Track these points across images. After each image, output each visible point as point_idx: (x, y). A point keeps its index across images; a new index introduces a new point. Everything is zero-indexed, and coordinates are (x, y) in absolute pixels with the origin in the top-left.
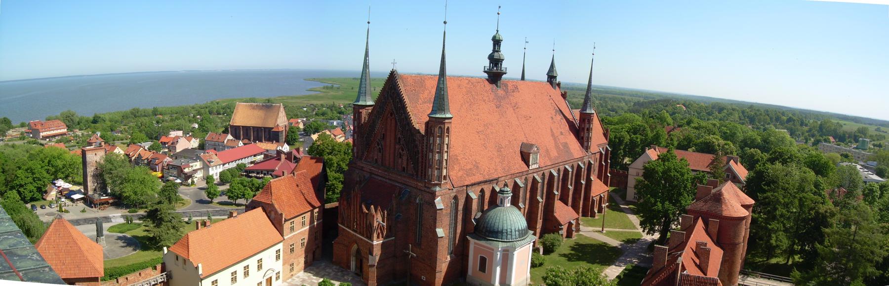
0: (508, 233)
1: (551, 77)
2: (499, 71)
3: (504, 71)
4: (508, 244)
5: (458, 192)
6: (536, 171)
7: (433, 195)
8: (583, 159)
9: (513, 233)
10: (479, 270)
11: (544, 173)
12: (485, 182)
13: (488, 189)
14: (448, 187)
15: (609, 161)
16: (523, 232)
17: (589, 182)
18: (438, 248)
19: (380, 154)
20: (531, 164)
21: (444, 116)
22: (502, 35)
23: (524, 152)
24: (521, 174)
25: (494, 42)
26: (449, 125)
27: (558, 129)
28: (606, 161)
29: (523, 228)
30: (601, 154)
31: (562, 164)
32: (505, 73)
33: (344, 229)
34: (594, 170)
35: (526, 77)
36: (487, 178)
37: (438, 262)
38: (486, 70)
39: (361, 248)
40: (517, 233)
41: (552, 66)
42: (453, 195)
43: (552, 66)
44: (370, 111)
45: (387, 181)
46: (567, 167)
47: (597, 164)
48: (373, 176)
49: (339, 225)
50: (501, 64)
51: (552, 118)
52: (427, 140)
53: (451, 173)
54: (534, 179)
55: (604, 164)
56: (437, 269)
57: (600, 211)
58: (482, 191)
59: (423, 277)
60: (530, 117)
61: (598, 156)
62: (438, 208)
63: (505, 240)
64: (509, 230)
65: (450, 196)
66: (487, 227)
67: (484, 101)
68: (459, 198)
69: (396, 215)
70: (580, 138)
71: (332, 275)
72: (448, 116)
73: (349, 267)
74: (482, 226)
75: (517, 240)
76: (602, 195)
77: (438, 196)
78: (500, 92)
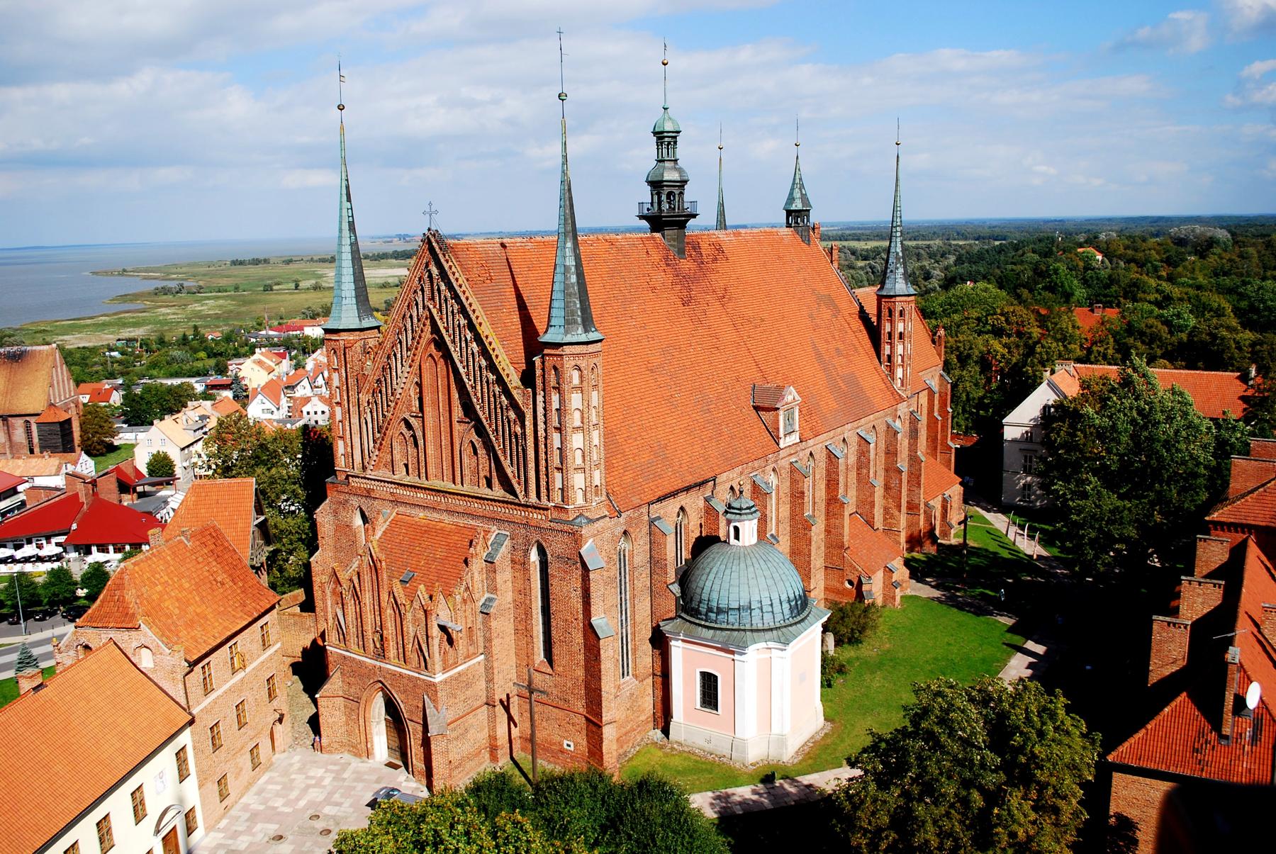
0: (764, 611)
1: (796, 217)
8: (896, 410)
9: (777, 608)
14: (607, 513)
18: (603, 667)
20: (781, 434)
24: (762, 462)
25: (659, 138)
26: (595, 360)
27: (827, 341)
28: (943, 412)
29: (797, 594)
32: (694, 216)
33: (345, 657)
36: (691, 480)
38: (646, 212)
40: (786, 606)
41: (797, 183)
43: (797, 183)
45: (446, 518)
48: (402, 509)
50: (681, 193)
51: (811, 316)
52: (544, 402)
55: (940, 418)
59: (566, 742)
60: (763, 320)
63: (760, 626)
64: (766, 602)
66: (709, 600)
69: (483, 601)
70: (883, 358)
71: (326, 782)
72: (593, 336)
73: (369, 754)
74: (697, 598)
78: (686, 265)
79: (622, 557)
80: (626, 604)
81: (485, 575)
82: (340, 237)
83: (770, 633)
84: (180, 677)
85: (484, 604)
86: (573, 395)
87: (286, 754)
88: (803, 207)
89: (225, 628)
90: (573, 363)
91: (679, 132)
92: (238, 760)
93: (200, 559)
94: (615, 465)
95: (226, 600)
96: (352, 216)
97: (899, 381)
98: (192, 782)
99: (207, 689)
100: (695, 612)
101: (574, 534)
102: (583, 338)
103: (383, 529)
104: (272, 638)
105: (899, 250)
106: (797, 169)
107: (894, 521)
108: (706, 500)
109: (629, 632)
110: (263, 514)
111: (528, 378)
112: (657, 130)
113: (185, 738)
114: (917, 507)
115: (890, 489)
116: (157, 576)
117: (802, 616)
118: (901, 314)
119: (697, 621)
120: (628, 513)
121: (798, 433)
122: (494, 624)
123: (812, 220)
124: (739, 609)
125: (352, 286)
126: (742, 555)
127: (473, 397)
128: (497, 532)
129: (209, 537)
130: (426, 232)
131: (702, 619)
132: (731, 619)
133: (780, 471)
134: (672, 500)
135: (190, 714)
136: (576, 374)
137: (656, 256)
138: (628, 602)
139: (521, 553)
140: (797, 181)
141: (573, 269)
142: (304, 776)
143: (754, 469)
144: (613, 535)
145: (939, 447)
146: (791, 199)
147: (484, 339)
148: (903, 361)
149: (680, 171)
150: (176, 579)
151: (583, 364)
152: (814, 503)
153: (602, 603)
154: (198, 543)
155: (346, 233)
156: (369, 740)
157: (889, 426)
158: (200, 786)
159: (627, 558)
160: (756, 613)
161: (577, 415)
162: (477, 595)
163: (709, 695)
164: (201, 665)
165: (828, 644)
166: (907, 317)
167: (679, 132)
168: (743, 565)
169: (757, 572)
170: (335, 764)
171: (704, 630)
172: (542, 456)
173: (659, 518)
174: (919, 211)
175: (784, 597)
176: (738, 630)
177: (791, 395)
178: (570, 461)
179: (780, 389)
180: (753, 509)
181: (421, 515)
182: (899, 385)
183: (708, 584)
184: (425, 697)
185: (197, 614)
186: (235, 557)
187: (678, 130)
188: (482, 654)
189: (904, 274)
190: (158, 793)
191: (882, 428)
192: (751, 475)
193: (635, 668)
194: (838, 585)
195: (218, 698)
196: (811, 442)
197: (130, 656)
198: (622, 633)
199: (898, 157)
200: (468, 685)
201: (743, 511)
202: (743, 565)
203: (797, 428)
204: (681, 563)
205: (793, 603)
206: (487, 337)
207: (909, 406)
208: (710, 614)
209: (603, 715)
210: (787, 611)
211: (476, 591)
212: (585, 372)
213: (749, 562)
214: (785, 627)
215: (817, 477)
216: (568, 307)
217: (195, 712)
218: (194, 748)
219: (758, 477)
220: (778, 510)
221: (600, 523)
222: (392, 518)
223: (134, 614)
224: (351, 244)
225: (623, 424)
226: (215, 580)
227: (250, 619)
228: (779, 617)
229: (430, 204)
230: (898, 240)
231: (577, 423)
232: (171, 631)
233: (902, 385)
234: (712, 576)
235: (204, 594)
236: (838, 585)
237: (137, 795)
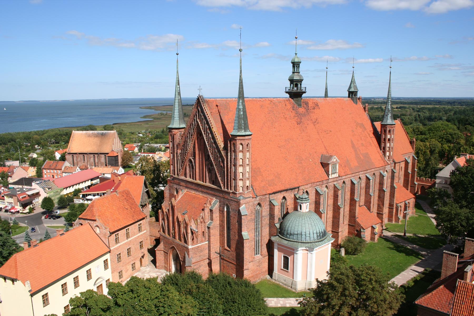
0: (307, 236)
1: (352, 94)
2: (299, 91)
3: (304, 90)
4: (307, 245)
5: (261, 199)
6: (336, 179)
7: (238, 203)
8: (385, 168)
9: (312, 235)
10: (283, 268)
11: (344, 181)
12: (287, 190)
13: (290, 196)
14: (251, 196)
15: (416, 170)
17: (393, 189)
18: (244, 249)
20: (330, 173)
21: (244, 133)
23: (324, 163)
24: (321, 183)
26: (248, 142)
29: (321, 231)
30: (407, 163)
31: (362, 173)
32: (305, 92)
34: (399, 179)
35: (329, 95)
36: (288, 187)
37: (245, 261)
38: (287, 90)
40: (315, 235)
41: (353, 82)
42: (257, 202)
43: (353, 82)
44: (183, 132)
46: (368, 176)
47: (402, 173)
50: (301, 84)
53: (254, 184)
54: (335, 187)
55: (410, 173)
56: (244, 268)
57: (405, 216)
58: (284, 198)
59: (233, 275)
60: (331, 131)
61: (403, 165)
62: (242, 215)
63: (304, 241)
64: (308, 233)
65: (254, 204)
66: (287, 230)
67: (286, 118)
68: (262, 205)
69: (209, 223)
75: (315, 241)
76: (407, 202)
77: (242, 204)
78: (301, 110)
79: (258, 212)
80: (259, 229)
81: (210, 214)
82: (175, 97)
84: (107, 237)
85: (209, 224)
86: (239, 154)
87: (145, 267)
88: (354, 90)
89: (125, 223)
90: (240, 142)
91: (300, 62)
92: (127, 267)
93: (121, 201)
94: (258, 180)
95: (127, 214)
97: (387, 157)
98: (109, 270)
99: (117, 241)
101: (238, 202)
102: (244, 134)
103: (181, 196)
104: (143, 229)
105: (389, 107)
106: (353, 76)
107: (381, 210)
108: (295, 195)
109: (260, 239)
110: (147, 188)
111: (225, 148)
112: (292, 61)
113: (108, 256)
114: (393, 205)
115: (380, 197)
116: (105, 204)
117: (322, 239)
118: (389, 131)
119: (283, 237)
120: (260, 197)
121: (338, 174)
122: (211, 231)
124: (297, 234)
125: (178, 114)
127: (209, 153)
128: (215, 200)
129: (125, 194)
130: (198, 96)
131: (285, 237)
132: (294, 238)
133: (329, 187)
134: (279, 194)
135: (110, 249)
136: (241, 146)
137: (289, 106)
138: (260, 228)
139: (222, 207)
140: (353, 81)
142: (148, 275)
143: (317, 185)
144: (254, 204)
145: (410, 184)
146: (350, 87)
147: (214, 133)
148: (389, 149)
149: (301, 76)
150: (111, 206)
151: (243, 143)
152: (345, 200)
153: (246, 227)
154: (121, 195)
155: (177, 96)
156: (170, 266)
157: (381, 174)
158: (112, 273)
159: (260, 213)
160: (304, 236)
161: (241, 160)
162: (206, 221)
163: (286, 265)
164: (115, 234)
165: (342, 252)
166: (392, 132)
167: (300, 62)
170: (159, 273)
171: (285, 241)
172: (229, 174)
173: (273, 200)
174: (396, 94)
175: (315, 232)
177: (334, 159)
178: (238, 177)
179: (331, 157)
181: (194, 192)
182: (387, 158)
183: (288, 224)
184: (186, 253)
185: (117, 218)
186: (133, 201)
187: (300, 61)
188: (207, 241)
189: (391, 117)
191: (377, 174)
192: (316, 187)
193: (261, 252)
194: (353, 231)
195: (121, 245)
196: (344, 177)
197: (93, 228)
198: (257, 239)
199: (390, 72)
200: (201, 251)
201: (303, 199)
202: (301, 219)
203: (337, 171)
205: (318, 234)
206: (214, 132)
207: (391, 167)
208: (287, 235)
209: (244, 266)
211: (206, 219)
212: (244, 146)
213: (303, 218)
214: (314, 242)
215: (346, 190)
216: (239, 123)
217: (112, 249)
218: (111, 260)
219: (319, 188)
220: (327, 201)
221: (249, 199)
222: (185, 192)
223: (95, 215)
224: (178, 100)
225: (264, 165)
226: (125, 208)
227: (134, 221)
228: (312, 239)
229: (200, 86)
231: (241, 164)
232: (106, 222)
233: (389, 158)
234: (290, 222)
235: (120, 212)
236: (353, 231)
237: (89, 273)
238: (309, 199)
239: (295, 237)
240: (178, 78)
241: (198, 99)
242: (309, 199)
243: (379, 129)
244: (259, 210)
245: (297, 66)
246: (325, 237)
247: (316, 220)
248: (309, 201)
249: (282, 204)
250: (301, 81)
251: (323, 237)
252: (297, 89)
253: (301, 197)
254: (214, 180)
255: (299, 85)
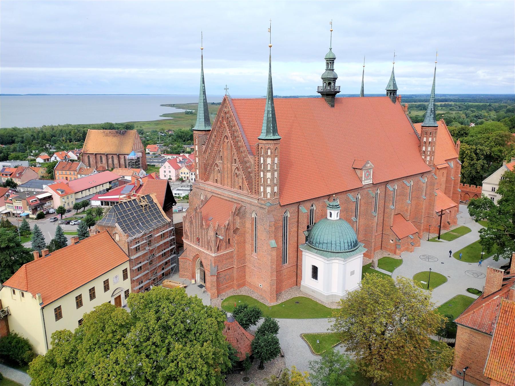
1: (392, 92)
3: (338, 90)
9: (342, 245)
16: (353, 244)
19: (219, 175)
20: (363, 180)
22: (336, 52)
29: (352, 240)
32: (339, 92)
38: (320, 90)
39: (203, 261)
40: (346, 244)
41: (393, 79)
43: (393, 79)
49: (184, 241)
59: (260, 284)
64: (338, 242)
75: (346, 251)
83: (338, 254)
88: (394, 88)
91: (335, 58)
96: (205, 89)
98: (128, 280)
100: (311, 243)
102: (272, 138)
117: (353, 249)
119: (312, 246)
123: (397, 94)
126: (331, 223)
131: (313, 245)
141: (271, 112)
146: (389, 85)
148: (430, 154)
152: (379, 208)
168: (331, 227)
169: (336, 230)
176: (326, 251)
180: (338, 206)
183: (317, 233)
190: (114, 283)
201: (334, 207)
202: (331, 227)
203: (371, 178)
204: (313, 224)
205: (350, 244)
208: (316, 244)
210: (346, 246)
224: (204, 100)
228: (343, 248)
229: (226, 86)
230: (433, 103)
233: (429, 163)
234: (319, 230)
238: (340, 207)
239: (325, 246)
240: (203, 76)
241: (225, 100)
242: (340, 207)
243: (419, 131)
244: (287, 217)
245: (331, 63)
246: (356, 247)
247: (347, 229)
248: (340, 208)
249: (311, 211)
250: (335, 79)
251: (354, 247)
252: (330, 87)
253: (331, 204)
254: (241, 185)
255: (333, 83)
